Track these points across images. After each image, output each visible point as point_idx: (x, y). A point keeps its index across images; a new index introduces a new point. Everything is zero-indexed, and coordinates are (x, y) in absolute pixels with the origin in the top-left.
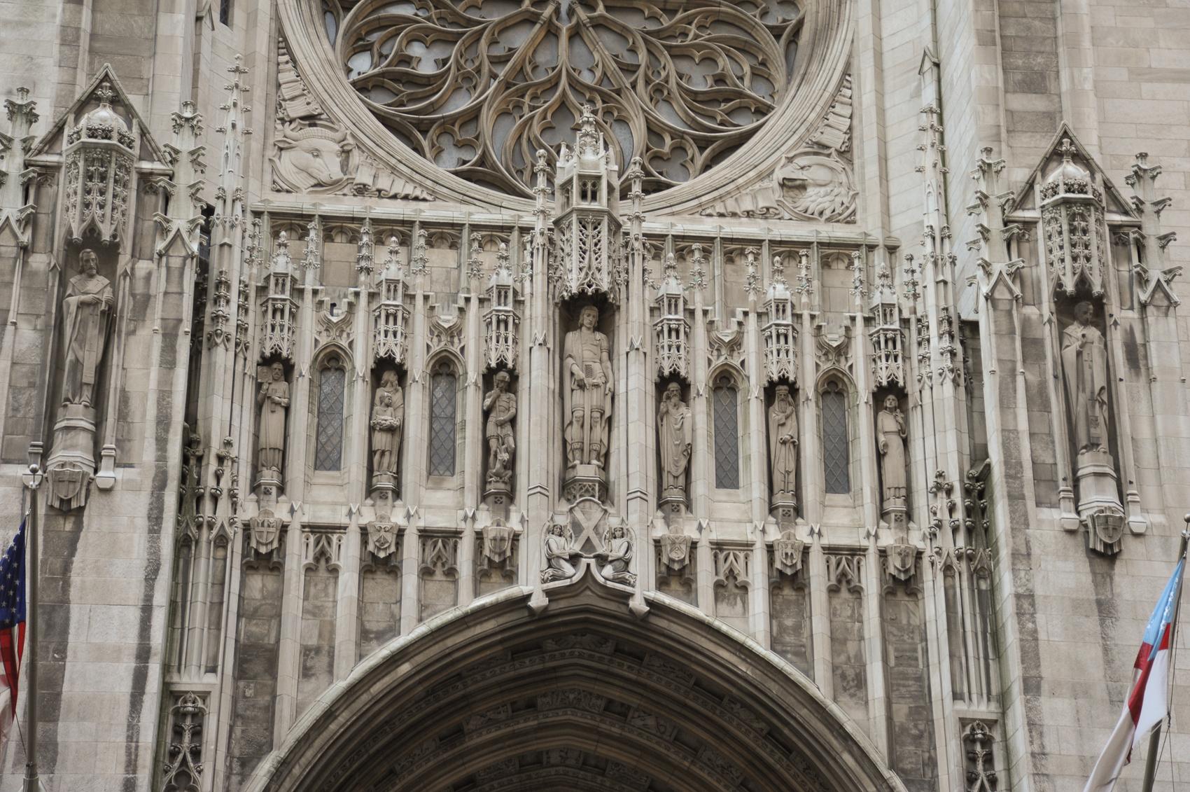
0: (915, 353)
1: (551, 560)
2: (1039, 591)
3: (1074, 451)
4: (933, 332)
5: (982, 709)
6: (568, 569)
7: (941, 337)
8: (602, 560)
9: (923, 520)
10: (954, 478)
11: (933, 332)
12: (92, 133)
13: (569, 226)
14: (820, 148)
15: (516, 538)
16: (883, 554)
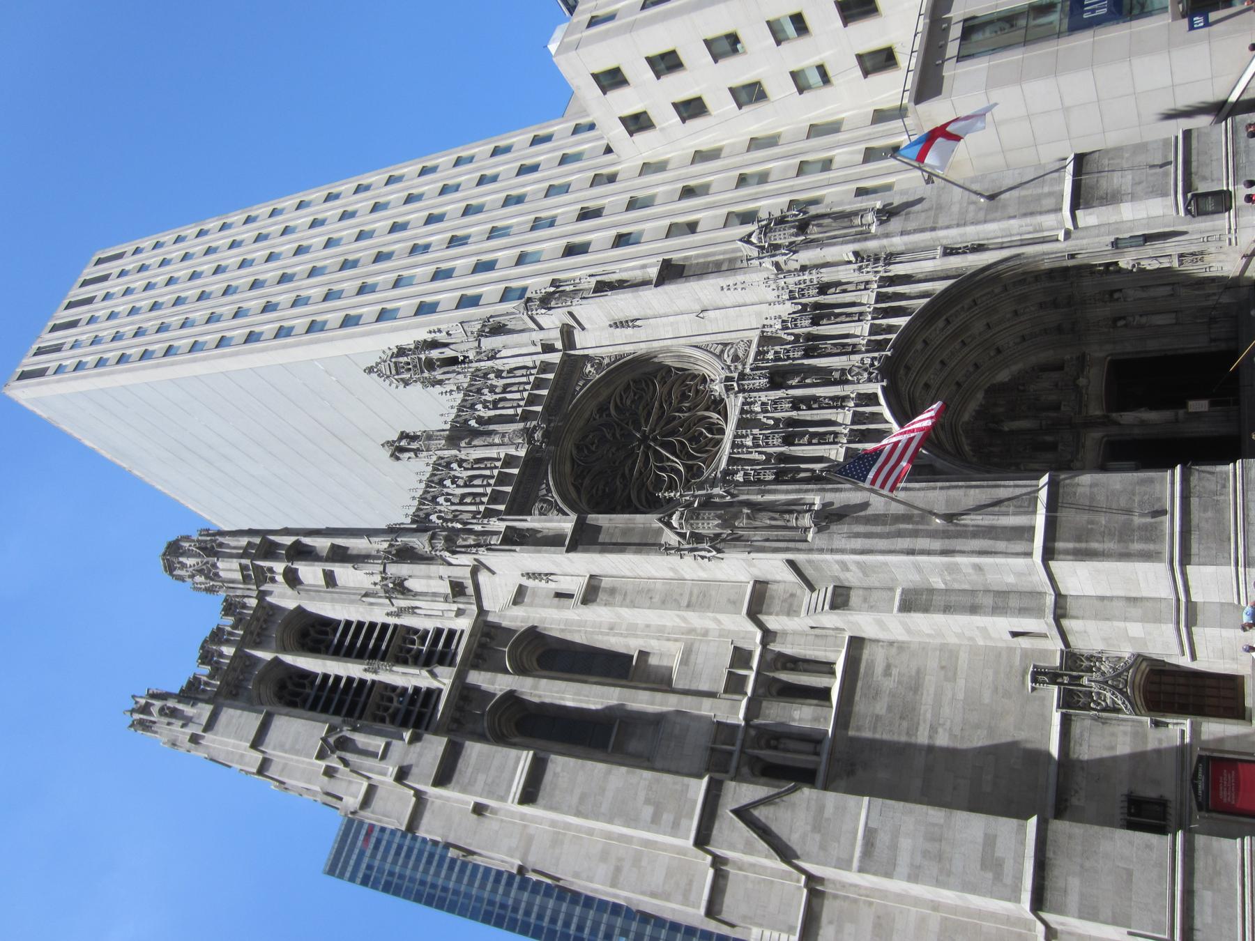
0: (808, 283)
1: (869, 380)
2: (900, 230)
3: (852, 227)
4: (801, 278)
5: (939, 251)
6: (874, 374)
7: (804, 275)
8: (872, 365)
9: (870, 277)
10: (855, 266)
11: (801, 278)
12: (681, 518)
13: (743, 385)
14: (722, 352)
15: (859, 394)
16: (879, 287)
